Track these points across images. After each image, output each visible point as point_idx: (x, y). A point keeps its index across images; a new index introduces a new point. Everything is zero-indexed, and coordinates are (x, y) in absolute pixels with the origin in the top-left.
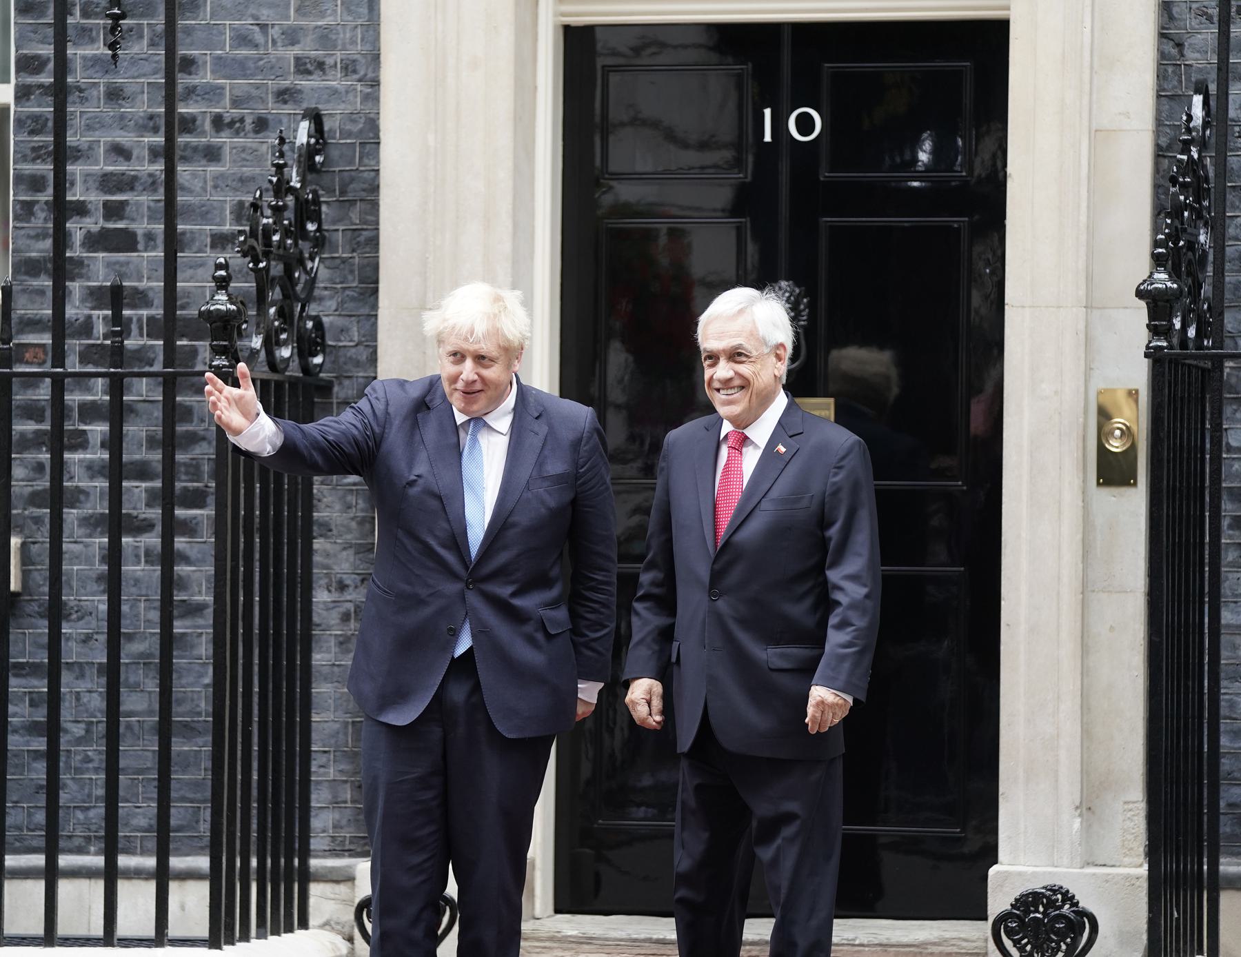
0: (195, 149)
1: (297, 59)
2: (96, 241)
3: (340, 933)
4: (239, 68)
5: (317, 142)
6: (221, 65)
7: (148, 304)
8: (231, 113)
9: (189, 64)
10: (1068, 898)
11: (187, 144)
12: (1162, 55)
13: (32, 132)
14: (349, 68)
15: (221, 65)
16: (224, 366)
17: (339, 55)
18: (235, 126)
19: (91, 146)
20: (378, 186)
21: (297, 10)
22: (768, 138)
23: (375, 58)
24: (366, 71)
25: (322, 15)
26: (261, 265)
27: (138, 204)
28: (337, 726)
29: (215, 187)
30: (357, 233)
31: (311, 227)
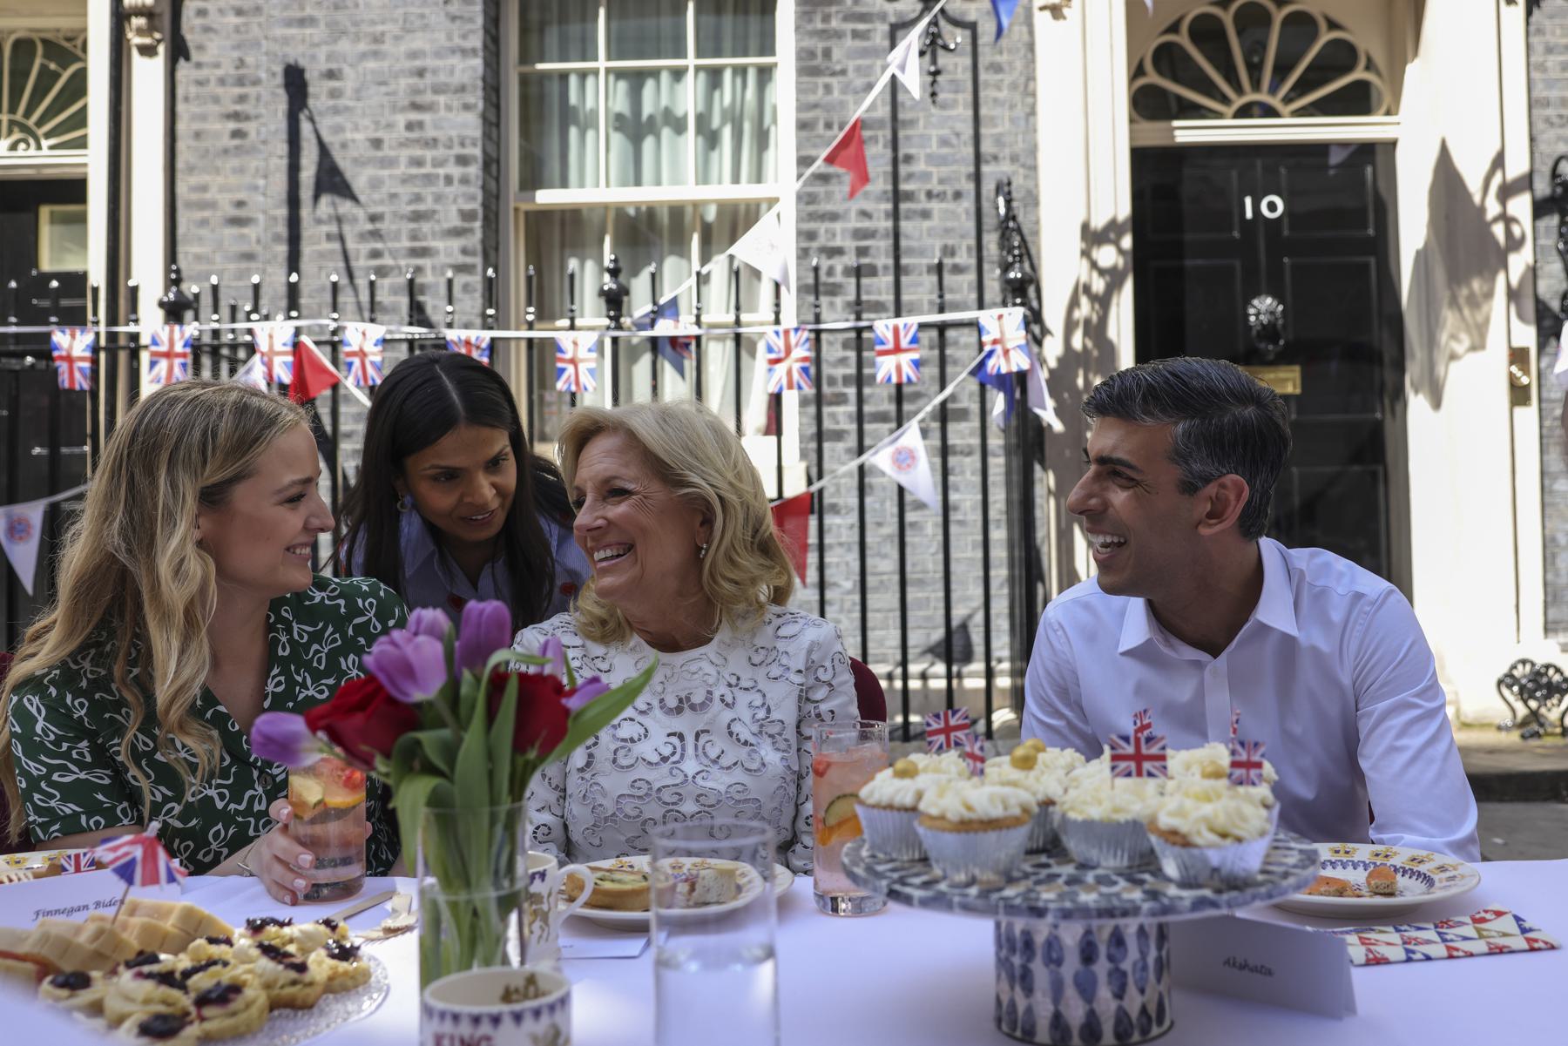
0: (915, 212)
2: (847, 272)
4: (942, 161)
6: (930, 159)
8: (937, 188)
9: (909, 159)
11: (909, 210)
13: (808, 203)
14: (1014, 159)
15: (930, 159)
17: (1007, 151)
18: (941, 196)
19: (847, 211)
23: (1033, 151)
25: (995, 126)
27: (878, 248)
29: (929, 235)
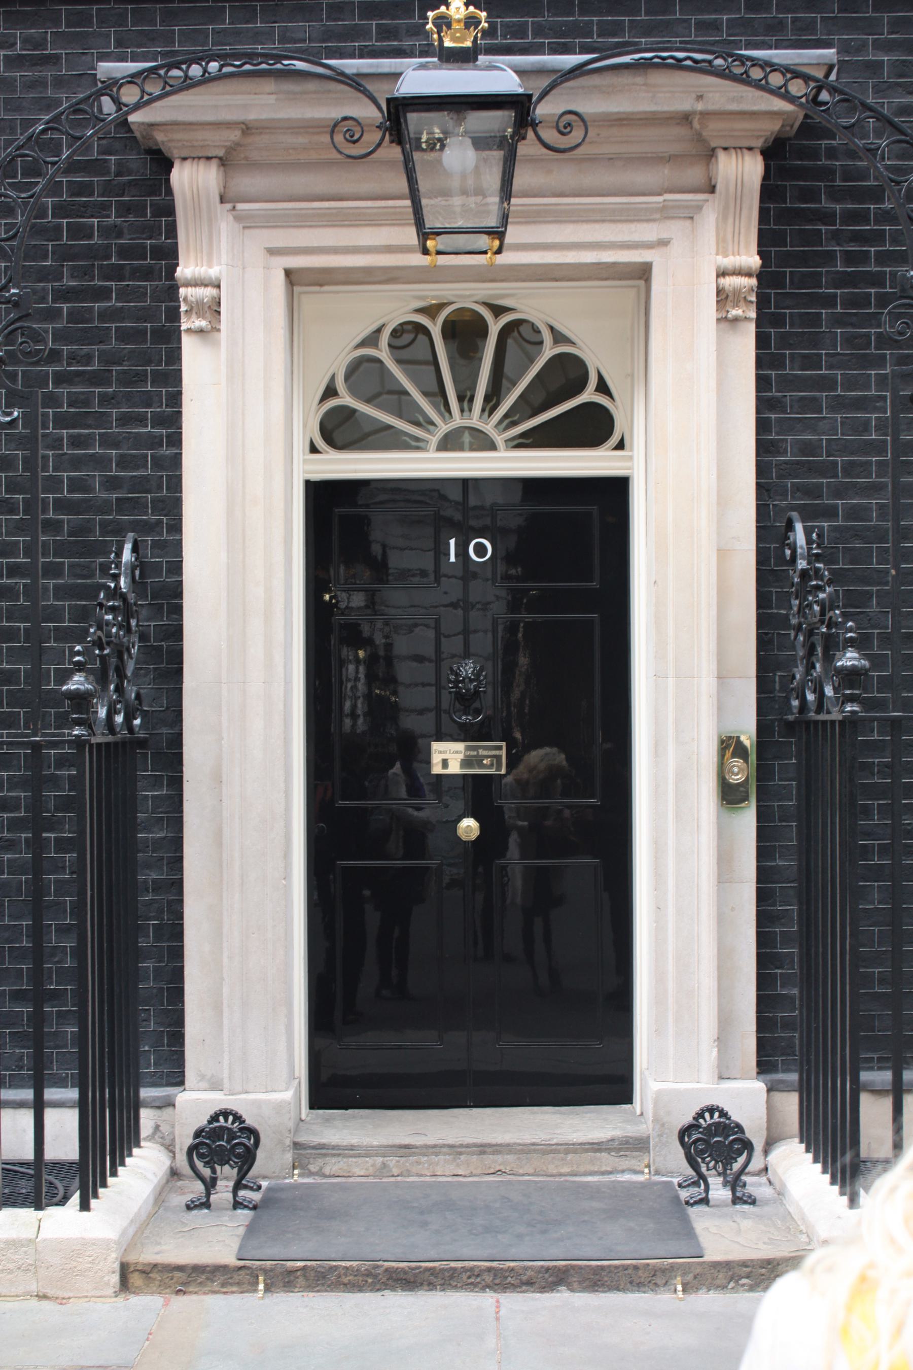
1: (117, 499)
3: (162, 1145)
5: (136, 559)
6: (60, 505)
7: (8, 682)
10: (723, 1114)
12: (758, 498)
15: (60, 505)
16: (83, 735)
20: (181, 593)
21: (116, 466)
22: (453, 559)
24: (171, 508)
25: (136, 468)
26: (106, 652)
28: (155, 991)
30: (164, 628)
31: (133, 622)
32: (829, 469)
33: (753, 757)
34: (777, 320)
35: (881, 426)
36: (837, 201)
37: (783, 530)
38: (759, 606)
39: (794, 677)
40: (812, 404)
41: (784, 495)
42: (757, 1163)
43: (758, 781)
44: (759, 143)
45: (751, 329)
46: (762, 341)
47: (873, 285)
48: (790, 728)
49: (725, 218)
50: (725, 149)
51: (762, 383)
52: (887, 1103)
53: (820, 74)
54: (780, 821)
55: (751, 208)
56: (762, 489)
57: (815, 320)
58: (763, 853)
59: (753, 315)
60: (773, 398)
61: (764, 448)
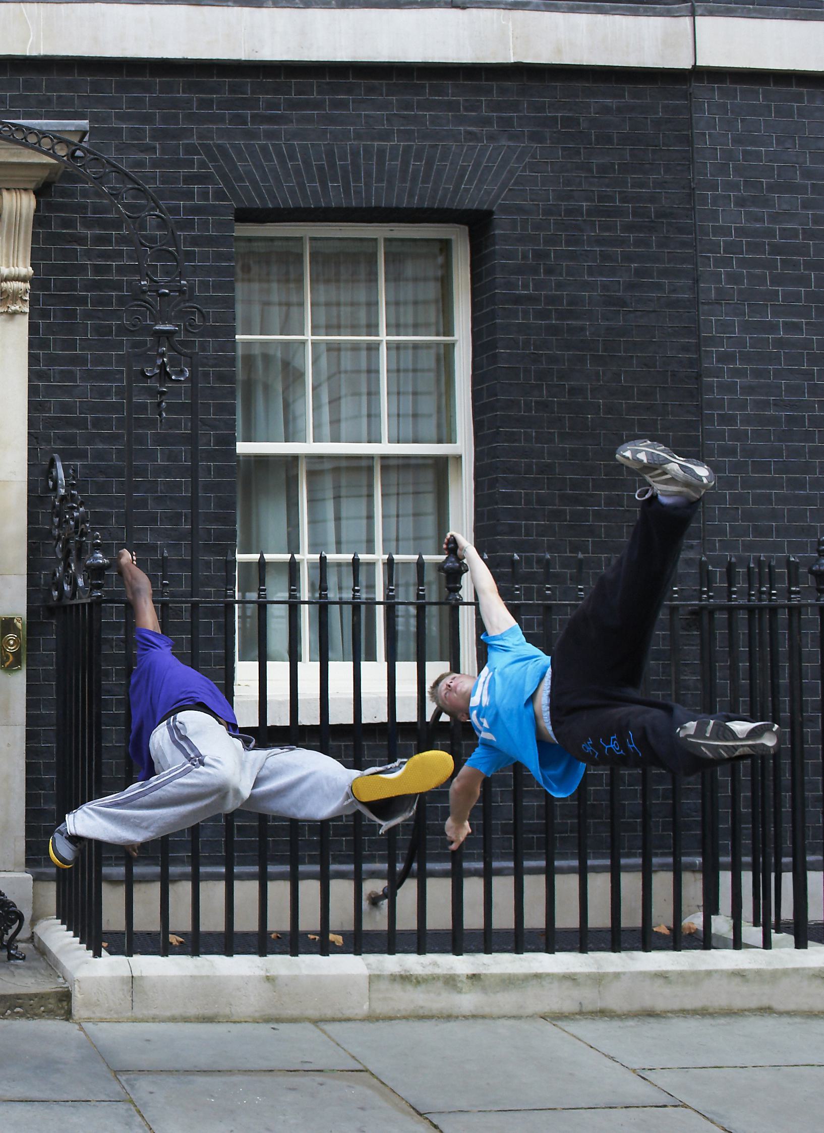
32: (81, 423)
33: (24, 633)
34: (45, 314)
35: (120, 392)
36: (88, 228)
37: (47, 466)
38: (29, 523)
39: (55, 575)
40: (70, 376)
41: (48, 442)
42: (24, 934)
43: (28, 651)
44: (32, 186)
45: (25, 320)
46: (33, 329)
47: (114, 289)
48: (51, 611)
49: (8, 239)
50: (8, 189)
51: (33, 359)
52: (121, 890)
53: (75, 139)
54: (44, 680)
55: (26, 233)
56: (33, 438)
57: (72, 314)
58: (31, 704)
59: (27, 310)
60: (41, 370)
61: (33, 407)
